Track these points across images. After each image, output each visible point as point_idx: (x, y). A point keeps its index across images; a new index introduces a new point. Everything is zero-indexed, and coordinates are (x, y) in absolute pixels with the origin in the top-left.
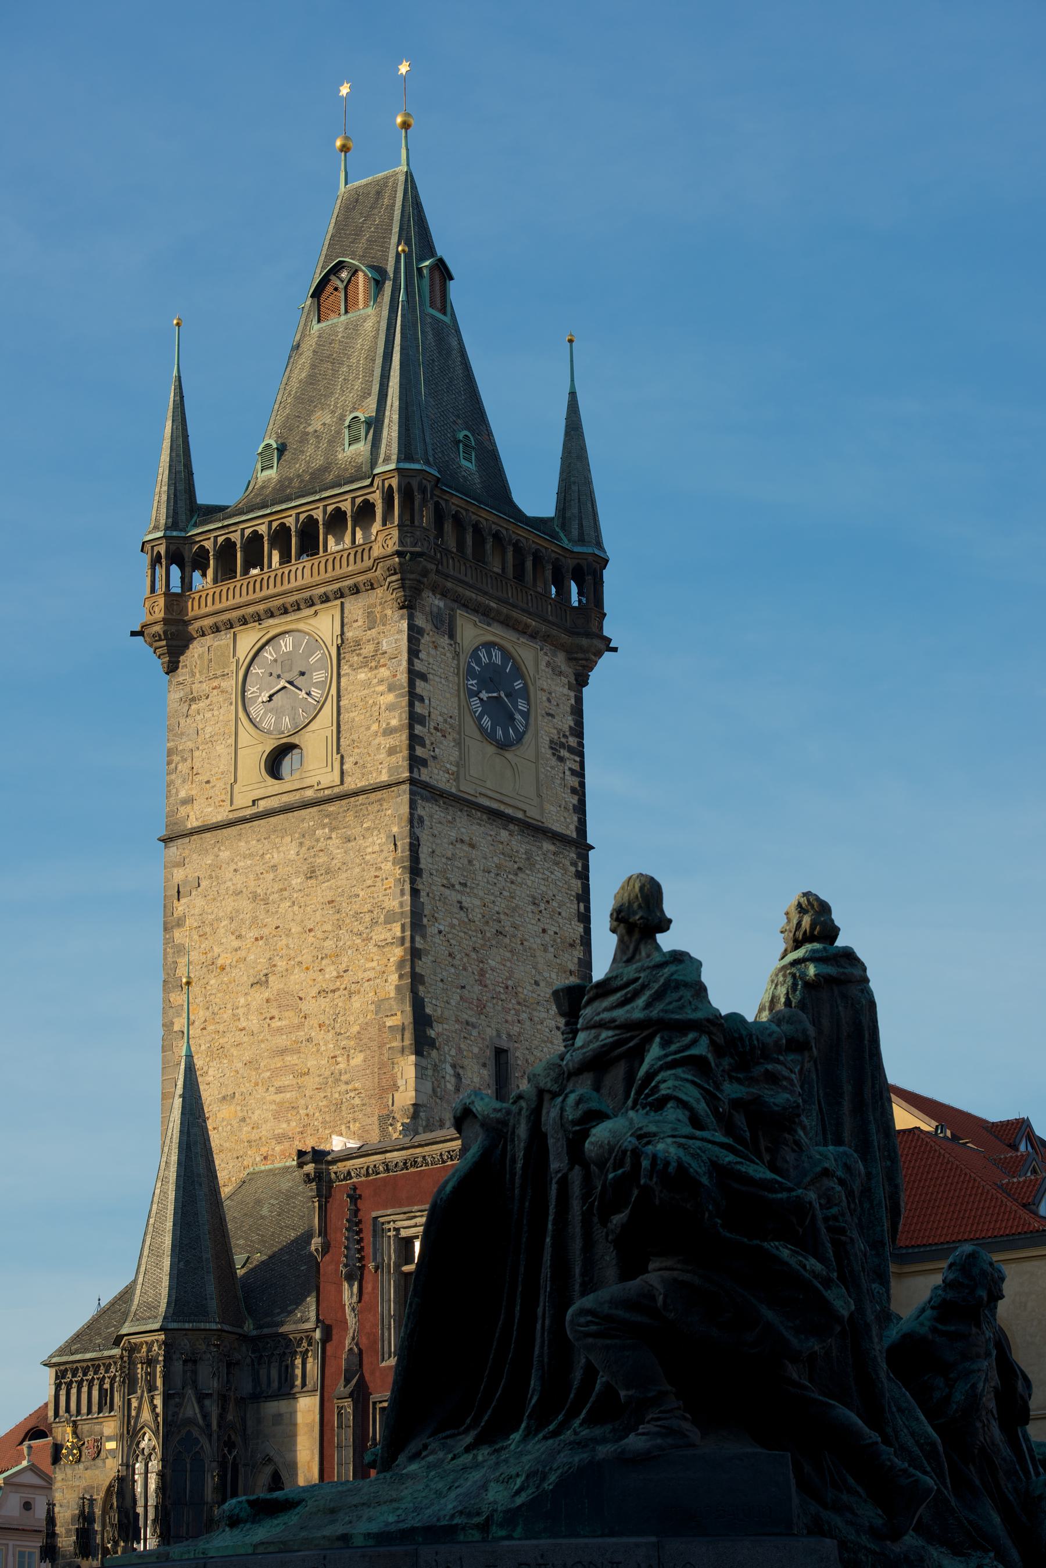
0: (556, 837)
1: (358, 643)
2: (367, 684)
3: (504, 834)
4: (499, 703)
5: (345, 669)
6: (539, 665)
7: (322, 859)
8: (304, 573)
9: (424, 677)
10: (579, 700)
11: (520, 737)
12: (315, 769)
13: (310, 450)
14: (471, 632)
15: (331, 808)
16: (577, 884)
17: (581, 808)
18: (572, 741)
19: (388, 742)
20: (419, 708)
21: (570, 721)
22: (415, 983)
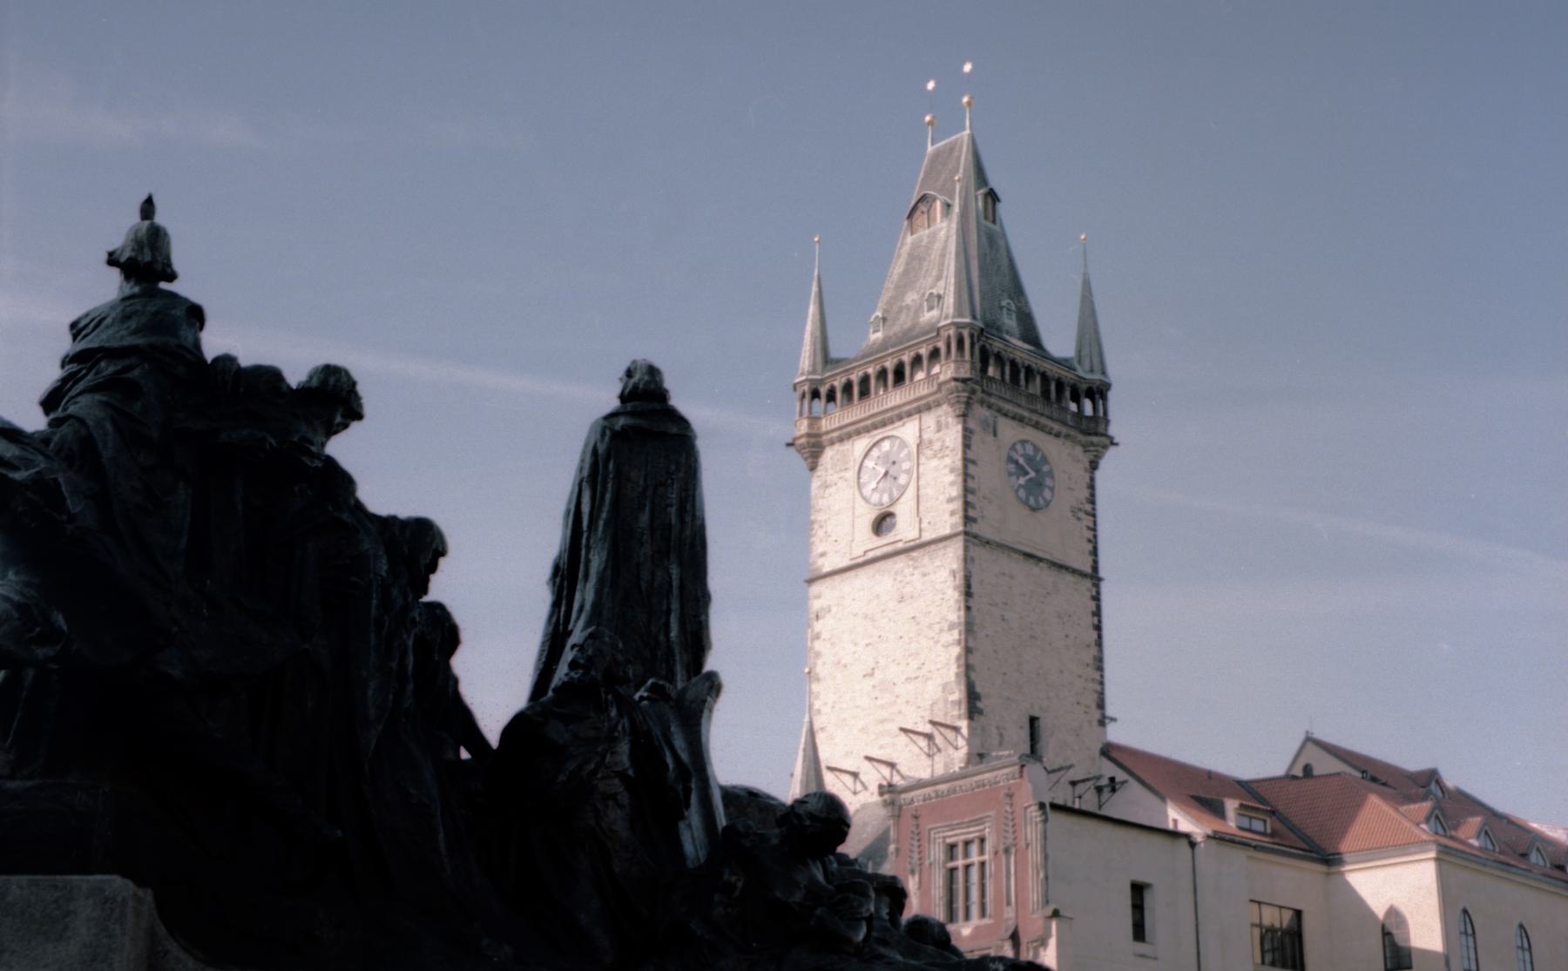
0: (1083, 575)
1: (931, 442)
2: (936, 469)
3: (1036, 570)
4: (1033, 481)
5: (923, 459)
6: (1062, 455)
7: (908, 589)
8: (895, 398)
9: (974, 462)
10: (1092, 479)
11: (1048, 503)
12: (905, 530)
13: (903, 317)
14: (1010, 432)
15: (914, 554)
16: (1092, 605)
17: (1095, 552)
18: (1088, 507)
19: (952, 506)
20: (971, 484)
21: (1086, 493)
22: (968, 670)
